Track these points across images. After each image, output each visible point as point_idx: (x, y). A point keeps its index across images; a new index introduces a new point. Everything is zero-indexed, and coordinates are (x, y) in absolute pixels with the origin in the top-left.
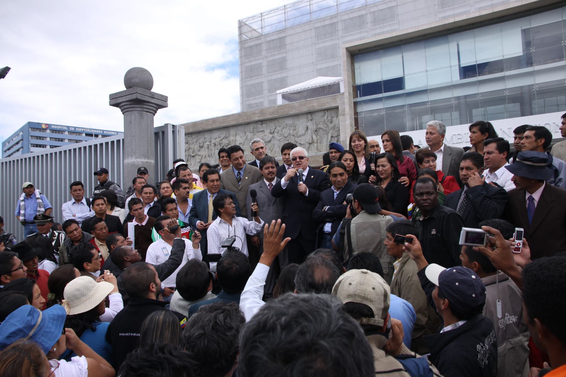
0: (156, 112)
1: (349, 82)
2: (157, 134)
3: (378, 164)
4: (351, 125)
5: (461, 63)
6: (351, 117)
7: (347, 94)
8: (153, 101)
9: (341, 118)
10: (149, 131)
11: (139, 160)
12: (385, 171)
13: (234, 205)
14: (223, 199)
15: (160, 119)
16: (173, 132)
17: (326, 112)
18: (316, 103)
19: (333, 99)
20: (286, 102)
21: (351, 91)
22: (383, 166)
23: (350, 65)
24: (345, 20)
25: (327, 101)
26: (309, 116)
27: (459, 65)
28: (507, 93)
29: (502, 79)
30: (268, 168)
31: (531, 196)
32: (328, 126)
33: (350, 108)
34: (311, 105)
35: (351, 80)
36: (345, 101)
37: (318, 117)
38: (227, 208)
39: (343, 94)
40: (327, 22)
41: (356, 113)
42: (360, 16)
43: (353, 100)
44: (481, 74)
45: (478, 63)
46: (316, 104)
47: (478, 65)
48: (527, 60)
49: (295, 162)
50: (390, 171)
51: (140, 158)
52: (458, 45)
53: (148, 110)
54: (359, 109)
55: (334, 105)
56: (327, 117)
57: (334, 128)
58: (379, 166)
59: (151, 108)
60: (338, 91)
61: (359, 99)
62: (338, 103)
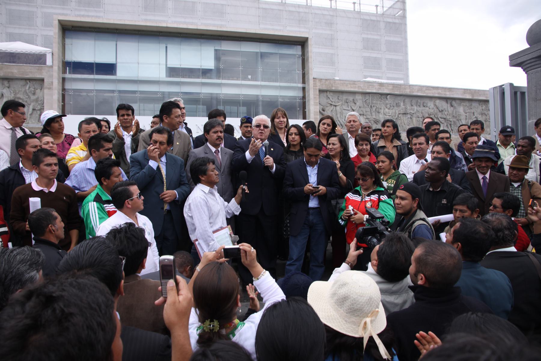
3: (330, 142)
4: (59, 101)
5: (168, 63)
6: (59, 92)
7: (56, 68)
9: (46, 91)
12: (335, 149)
13: (217, 173)
14: (206, 165)
17: (28, 82)
18: (15, 70)
19: (38, 70)
21: (61, 66)
22: (333, 144)
23: (61, 38)
25: (31, 71)
26: (6, 83)
27: (166, 65)
28: (202, 96)
29: (219, 85)
30: (216, 132)
31: (485, 176)
32: (29, 97)
33: (58, 83)
34: (9, 70)
35: (61, 55)
36: (52, 74)
37: (17, 86)
38: (210, 176)
39: (52, 67)
41: (64, 89)
43: (62, 76)
44: (178, 76)
45: (202, 68)
46: (15, 71)
47: (202, 69)
48: (218, 72)
49: (258, 129)
50: (339, 150)
54: (68, 86)
55: (38, 76)
56: (29, 87)
57: (37, 100)
58: (330, 144)
60: (45, 63)
61: (68, 76)
62: (43, 75)
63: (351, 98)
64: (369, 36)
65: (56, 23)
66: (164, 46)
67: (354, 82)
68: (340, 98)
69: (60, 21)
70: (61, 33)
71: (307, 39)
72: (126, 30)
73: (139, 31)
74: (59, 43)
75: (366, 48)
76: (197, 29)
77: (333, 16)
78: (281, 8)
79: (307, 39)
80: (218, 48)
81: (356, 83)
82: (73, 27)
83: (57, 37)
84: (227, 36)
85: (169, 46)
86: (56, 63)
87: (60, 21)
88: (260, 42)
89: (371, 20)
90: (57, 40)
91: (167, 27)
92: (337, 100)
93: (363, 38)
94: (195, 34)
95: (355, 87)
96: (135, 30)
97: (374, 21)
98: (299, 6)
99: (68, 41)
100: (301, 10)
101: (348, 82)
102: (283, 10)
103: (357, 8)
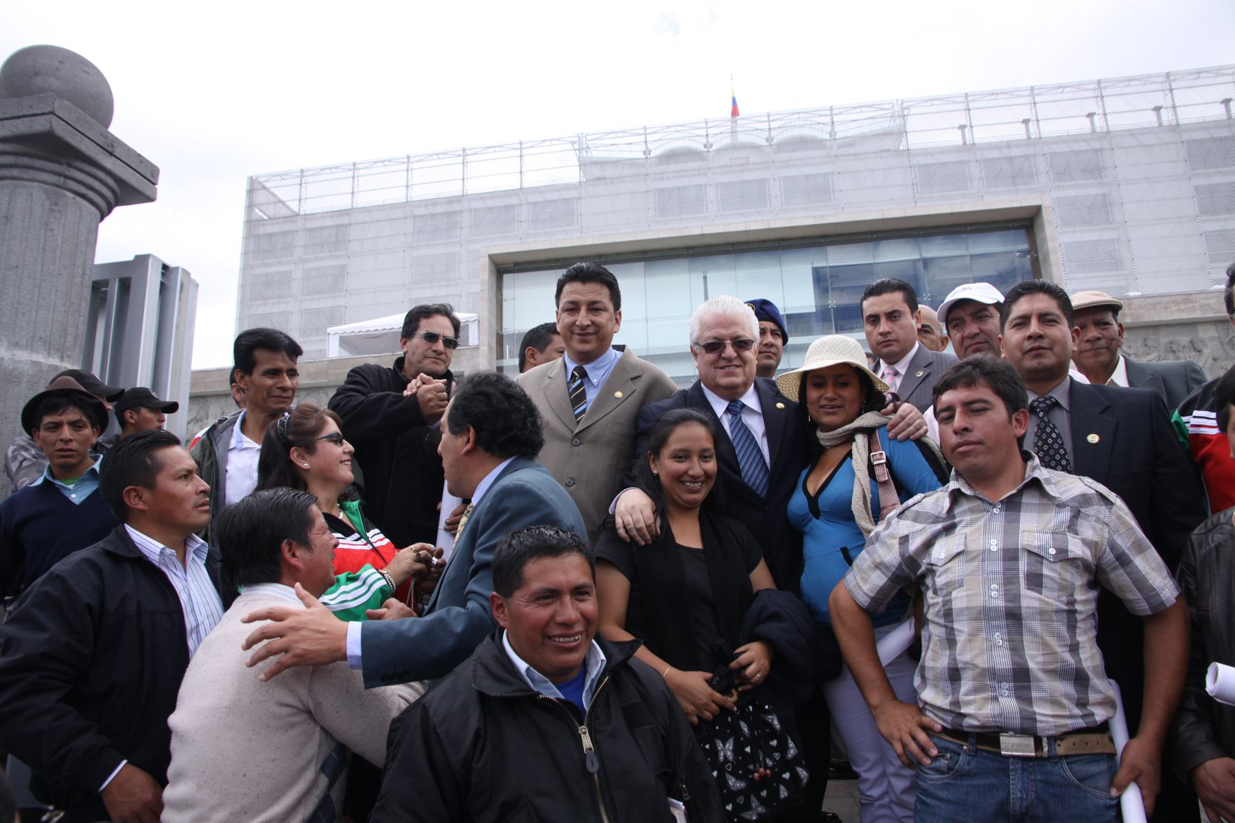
0: (110, 211)
1: (490, 325)
2: (99, 289)
7: (484, 349)
8: (109, 163)
10: (79, 262)
11: (23, 356)
15: (121, 236)
16: (162, 284)
20: (346, 354)
24: (476, 210)
35: (494, 321)
39: (477, 348)
40: (440, 209)
42: (507, 207)
51: (30, 347)
52: (705, 278)
53: (83, 190)
59: (97, 185)
63: (1184, 338)
64: (1215, 180)
65: (487, 259)
66: (701, 275)
67: (1187, 298)
68: (1150, 343)
69: (490, 256)
70: (494, 279)
71: (1037, 210)
72: (618, 254)
73: (644, 252)
74: (490, 301)
75: (1204, 211)
76: (769, 230)
77: (1101, 150)
78: (964, 157)
79: (1037, 210)
80: (816, 265)
81: (1193, 297)
82: (516, 264)
83: (486, 288)
84: (840, 235)
85: (709, 275)
86: (485, 338)
87: (490, 256)
88: (918, 236)
89: (1215, 140)
90: (486, 293)
91: (703, 235)
92: (1141, 350)
93: (1197, 188)
94: (765, 241)
95: (1193, 309)
96: (636, 252)
97: (1222, 139)
98: (1009, 145)
99: (507, 293)
100: (1015, 152)
101: (1169, 299)
102: (969, 162)
103: (1167, 116)
